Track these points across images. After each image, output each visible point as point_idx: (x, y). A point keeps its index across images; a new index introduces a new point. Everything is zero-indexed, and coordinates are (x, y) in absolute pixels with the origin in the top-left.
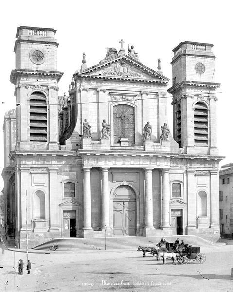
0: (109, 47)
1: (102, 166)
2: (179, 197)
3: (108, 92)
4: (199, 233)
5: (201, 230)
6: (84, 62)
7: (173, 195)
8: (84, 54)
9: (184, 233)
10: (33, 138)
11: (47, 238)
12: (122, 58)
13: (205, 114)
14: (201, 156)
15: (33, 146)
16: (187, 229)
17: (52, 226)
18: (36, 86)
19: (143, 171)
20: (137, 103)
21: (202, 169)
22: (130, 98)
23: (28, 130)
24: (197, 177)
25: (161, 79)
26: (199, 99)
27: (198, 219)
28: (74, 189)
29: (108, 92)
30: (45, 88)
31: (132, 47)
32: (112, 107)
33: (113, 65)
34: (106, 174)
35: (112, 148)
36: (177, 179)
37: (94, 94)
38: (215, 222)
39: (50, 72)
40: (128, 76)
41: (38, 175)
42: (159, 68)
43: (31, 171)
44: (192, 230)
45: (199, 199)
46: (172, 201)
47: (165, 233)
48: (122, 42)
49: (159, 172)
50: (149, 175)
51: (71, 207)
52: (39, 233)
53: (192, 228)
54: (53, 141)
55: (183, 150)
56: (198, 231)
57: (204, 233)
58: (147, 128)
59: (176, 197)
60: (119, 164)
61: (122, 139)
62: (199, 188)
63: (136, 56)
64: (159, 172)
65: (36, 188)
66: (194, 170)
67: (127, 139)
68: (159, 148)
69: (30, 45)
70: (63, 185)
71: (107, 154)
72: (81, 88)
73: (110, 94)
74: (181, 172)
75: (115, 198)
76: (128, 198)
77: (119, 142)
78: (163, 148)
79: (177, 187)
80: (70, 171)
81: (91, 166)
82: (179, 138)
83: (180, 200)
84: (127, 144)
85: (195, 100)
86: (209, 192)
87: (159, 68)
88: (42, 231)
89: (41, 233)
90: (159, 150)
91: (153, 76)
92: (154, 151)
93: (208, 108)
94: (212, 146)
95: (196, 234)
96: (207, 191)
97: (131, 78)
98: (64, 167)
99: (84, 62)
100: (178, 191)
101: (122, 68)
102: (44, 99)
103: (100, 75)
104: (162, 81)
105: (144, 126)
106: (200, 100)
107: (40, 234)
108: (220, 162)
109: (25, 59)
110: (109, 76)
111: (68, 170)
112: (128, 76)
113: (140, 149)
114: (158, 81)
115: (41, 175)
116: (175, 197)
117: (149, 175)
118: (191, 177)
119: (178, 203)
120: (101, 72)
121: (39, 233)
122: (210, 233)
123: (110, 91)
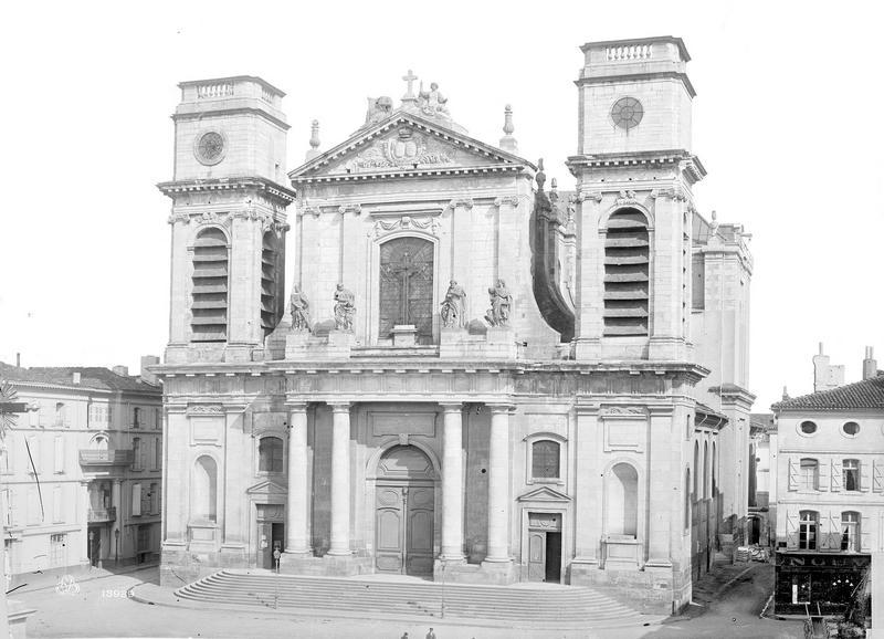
0: (376, 97)
1: (330, 400)
2: (551, 480)
3: (366, 212)
4: (606, 584)
5: (612, 575)
6: (314, 144)
7: (535, 475)
9: (562, 579)
10: (198, 336)
11: (215, 566)
12: (399, 122)
13: (643, 243)
14: (612, 366)
15: (196, 354)
16: (568, 570)
17: (230, 540)
18: (205, 215)
19: (436, 410)
21: (623, 401)
22: (421, 221)
23: (599, 295)
24: (607, 423)
25: (501, 160)
28: (273, 452)
29: (366, 212)
30: (646, 195)
33: (379, 142)
34: (342, 421)
35: (356, 353)
36: (546, 428)
37: (488, 216)
38: (658, 555)
39: (231, 181)
40: (415, 166)
41: (202, 420)
42: (508, 131)
43: (190, 410)
44: (583, 572)
45: (616, 487)
46: (532, 488)
47: (486, 576)
49: (473, 411)
50: (453, 423)
51: (266, 497)
52: (200, 553)
53: (583, 567)
54: (236, 340)
55: (566, 348)
56: (602, 577)
57: (623, 584)
58: (453, 296)
59: (542, 479)
60: (372, 393)
61: (397, 327)
62: (613, 456)
63: (445, 107)
64: (475, 412)
65: (200, 451)
66: (597, 405)
67: (412, 327)
68: (477, 347)
69: (196, 123)
70: (258, 443)
71: (332, 371)
72: (582, 196)
73: (373, 217)
74: (561, 409)
75: (382, 475)
76: (406, 477)
77: (392, 336)
78: (488, 347)
79: (547, 456)
80: (272, 410)
81: (301, 399)
82: (561, 320)
83: (554, 488)
84: (410, 341)
85: (610, 205)
86: (645, 468)
88: (205, 550)
89: (205, 553)
90: (477, 354)
91: (494, 155)
92: (463, 357)
93: (650, 225)
94: (657, 332)
95: (594, 584)
96: (640, 464)
97: (424, 167)
98: (262, 400)
100: (551, 462)
101: (401, 147)
102: (224, 244)
103: (349, 171)
104: (504, 167)
106: (623, 203)
107: (200, 557)
109: (185, 158)
110: (366, 171)
111: (268, 407)
112: (415, 166)
113: (429, 352)
114: (493, 167)
115: (210, 420)
116: (539, 479)
117: (453, 423)
118: (588, 423)
119: (545, 496)
120: (349, 164)
121: (200, 553)
122: (641, 586)
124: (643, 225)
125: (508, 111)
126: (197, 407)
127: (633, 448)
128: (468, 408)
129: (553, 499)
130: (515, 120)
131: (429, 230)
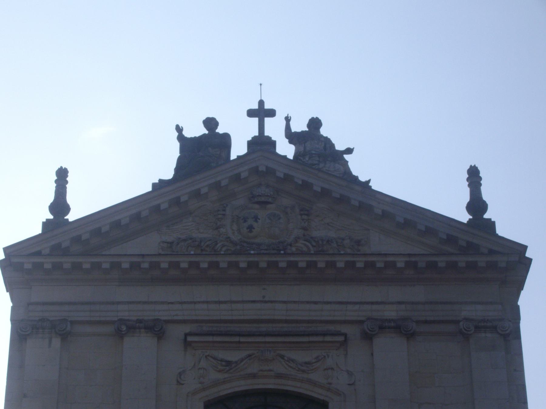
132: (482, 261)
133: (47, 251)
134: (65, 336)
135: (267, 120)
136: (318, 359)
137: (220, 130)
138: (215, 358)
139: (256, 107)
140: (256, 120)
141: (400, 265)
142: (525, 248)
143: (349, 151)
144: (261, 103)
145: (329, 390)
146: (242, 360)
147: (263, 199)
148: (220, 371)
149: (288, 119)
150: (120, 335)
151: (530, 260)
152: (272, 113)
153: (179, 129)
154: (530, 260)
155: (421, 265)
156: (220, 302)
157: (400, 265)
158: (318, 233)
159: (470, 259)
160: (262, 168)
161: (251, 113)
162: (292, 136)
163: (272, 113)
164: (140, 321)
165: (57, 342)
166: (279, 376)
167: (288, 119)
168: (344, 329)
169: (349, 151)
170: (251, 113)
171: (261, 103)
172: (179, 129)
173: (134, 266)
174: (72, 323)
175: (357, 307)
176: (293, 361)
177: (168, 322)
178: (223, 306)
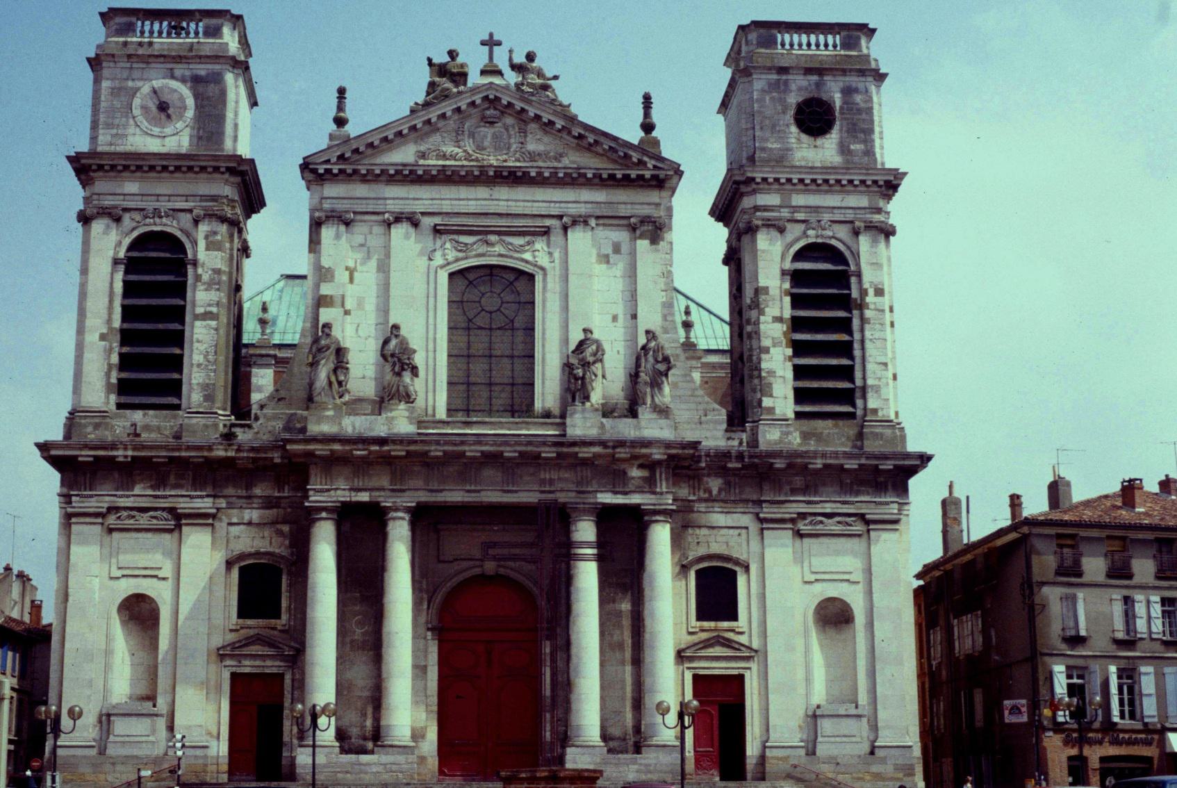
2: (725, 624)
3: (428, 222)
6: (340, 122)
8: (342, 92)
12: (486, 98)
20: (543, 260)
24: (806, 540)
25: (641, 163)
26: (811, 232)
27: (815, 716)
31: (530, 57)
32: (443, 277)
36: (716, 548)
42: (648, 127)
46: (695, 638)
48: (491, 43)
59: (712, 624)
62: (818, 587)
65: (128, 587)
85: (798, 237)
87: (648, 127)
93: (853, 268)
99: (340, 122)
105: (572, 347)
106: (812, 237)
108: (913, 482)
114: (633, 174)
116: (706, 624)
123: (437, 220)
124: (840, 268)
125: (647, 100)
126: (125, 514)
127: (846, 577)
128: (606, 517)
129: (730, 653)
130: (656, 116)
131: (527, 256)
132: (648, 174)
133: (334, 160)
134: (347, 224)
135: (496, 48)
136: (528, 243)
137: (460, 60)
138: (457, 242)
139: (487, 38)
140: (486, 48)
141: (590, 175)
142: (679, 165)
143: (556, 78)
144: (491, 35)
145: (536, 266)
146: (475, 243)
147: (491, 120)
148: (460, 251)
149: (511, 51)
150: (389, 225)
151: (683, 172)
152: (499, 44)
153: (430, 60)
154: (683, 172)
155: (605, 176)
156: (460, 200)
157: (590, 175)
158: (531, 146)
159: (641, 172)
160: (491, 97)
161: (483, 43)
162: (515, 67)
163: (499, 44)
164: (402, 213)
165: (342, 228)
166: (501, 255)
167: (511, 51)
168: (548, 222)
169: (556, 78)
170: (483, 43)
171: (491, 35)
172: (430, 60)
173: (397, 172)
174: (355, 213)
175: (557, 205)
176: (511, 244)
177: (423, 214)
178: (461, 202)
